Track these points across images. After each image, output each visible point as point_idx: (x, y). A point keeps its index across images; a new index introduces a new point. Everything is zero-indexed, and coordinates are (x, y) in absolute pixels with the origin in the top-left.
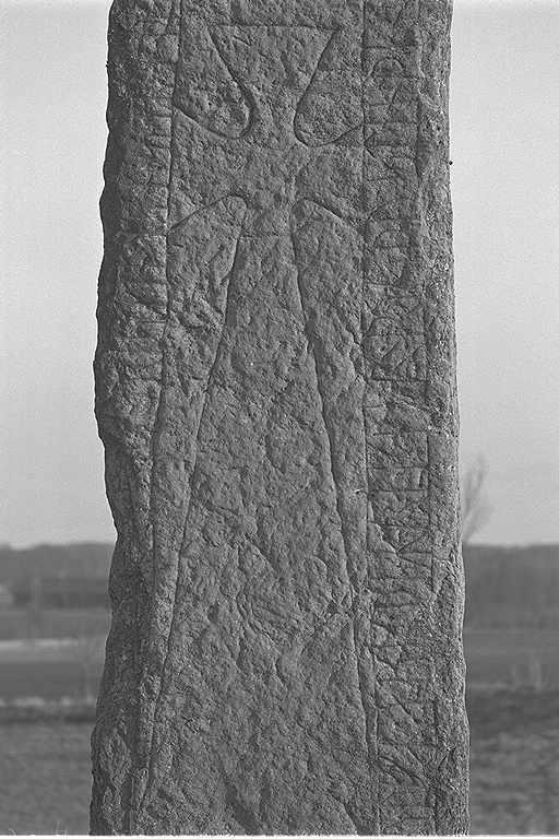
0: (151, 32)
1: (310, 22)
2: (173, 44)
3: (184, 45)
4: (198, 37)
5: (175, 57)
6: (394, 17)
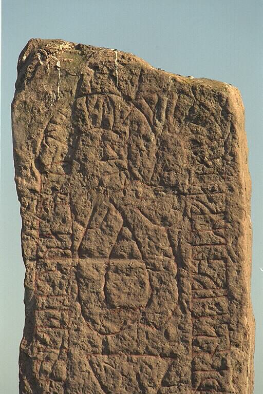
0: (48, 359)
1: (155, 351)
2: (63, 367)
3: (70, 367)
4: (80, 363)
5: (64, 376)
6: (213, 349)
